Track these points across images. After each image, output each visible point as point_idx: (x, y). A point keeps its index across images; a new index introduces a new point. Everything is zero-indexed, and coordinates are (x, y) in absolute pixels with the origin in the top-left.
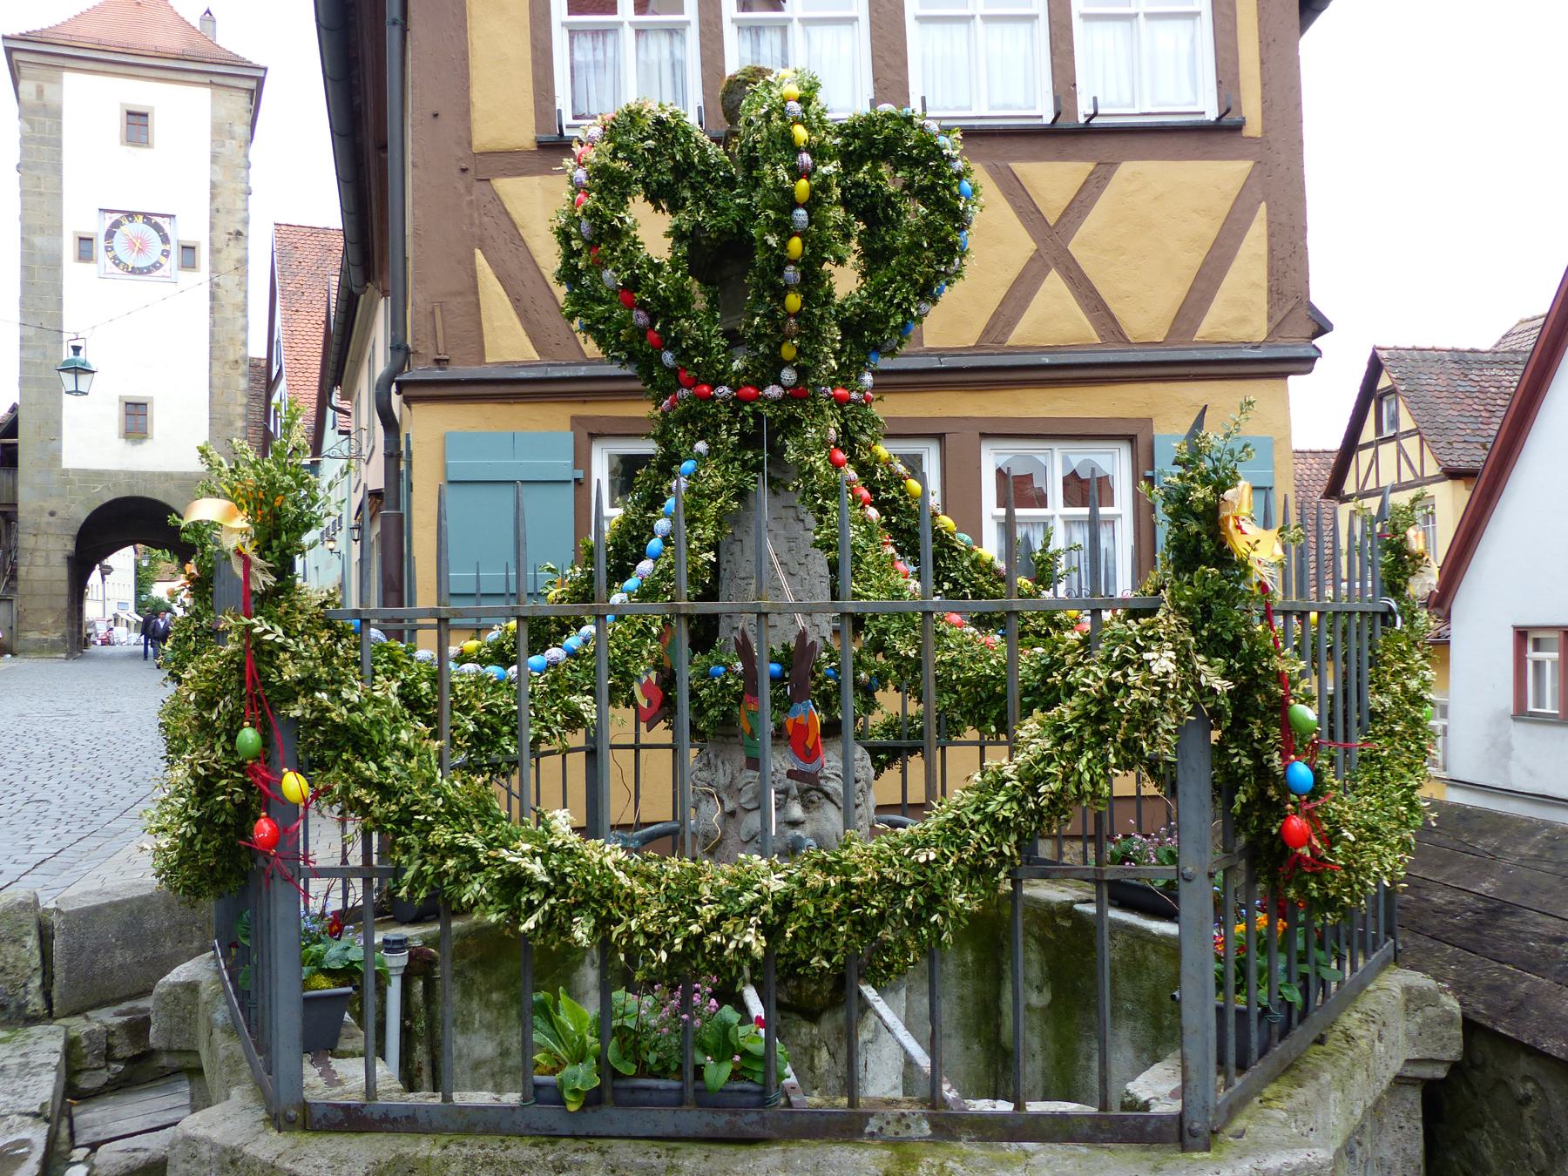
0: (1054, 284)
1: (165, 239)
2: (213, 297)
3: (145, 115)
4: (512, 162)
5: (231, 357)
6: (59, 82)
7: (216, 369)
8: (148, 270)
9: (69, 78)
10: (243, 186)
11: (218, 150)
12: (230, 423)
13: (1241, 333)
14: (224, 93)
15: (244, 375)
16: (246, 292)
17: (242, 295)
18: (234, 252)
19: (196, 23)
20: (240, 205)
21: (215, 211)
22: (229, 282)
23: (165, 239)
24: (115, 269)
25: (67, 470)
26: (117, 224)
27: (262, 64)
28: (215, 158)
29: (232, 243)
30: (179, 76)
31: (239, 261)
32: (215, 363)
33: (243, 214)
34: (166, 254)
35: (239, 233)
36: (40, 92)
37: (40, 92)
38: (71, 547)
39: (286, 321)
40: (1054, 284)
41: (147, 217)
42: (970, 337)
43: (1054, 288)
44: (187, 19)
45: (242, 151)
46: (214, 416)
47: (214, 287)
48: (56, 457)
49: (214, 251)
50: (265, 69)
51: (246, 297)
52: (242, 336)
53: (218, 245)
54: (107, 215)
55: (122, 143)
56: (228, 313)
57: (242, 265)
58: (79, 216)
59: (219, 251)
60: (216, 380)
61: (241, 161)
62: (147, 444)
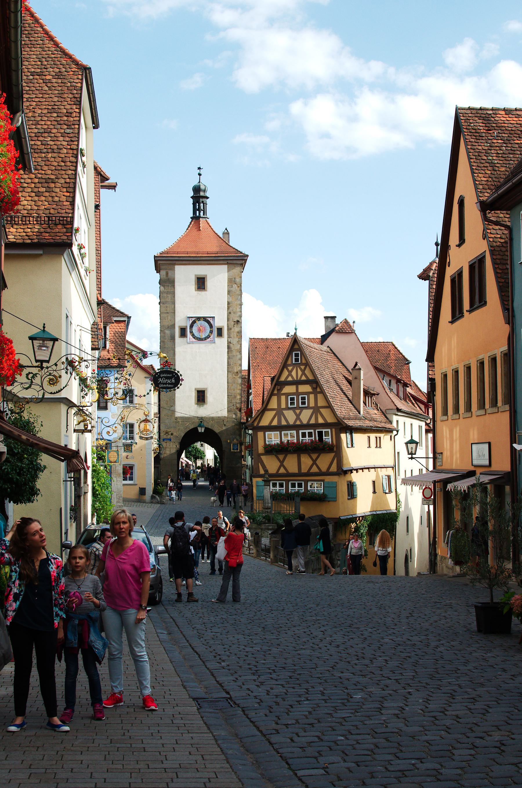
0: (315, 466)
1: (211, 326)
2: (229, 347)
3: (204, 278)
4: (262, 454)
5: (236, 371)
6: (174, 270)
7: (230, 376)
8: (205, 339)
9: (177, 267)
10: (239, 302)
11: (230, 289)
12: (235, 397)
13: (334, 471)
14: (231, 266)
15: (240, 377)
16: (241, 344)
17: (239, 346)
18: (236, 329)
19: (221, 236)
20: (238, 310)
21: (229, 313)
22: (235, 341)
23: (211, 326)
24: (194, 340)
25: (177, 418)
26: (194, 322)
27: (246, 254)
28: (229, 292)
29: (235, 326)
30: (216, 262)
31: (238, 332)
32: (229, 373)
33: (240, 313)
34: (211, 332)
35: (238, 321)
36: (167, 274)
37: (167, 274)
38: (178, 446)
39: (253, 377)
40: (315, 466)
41: (205, 319)
42: (306, 471)
43: (315, 466)
44: (218, 234)
45: (239, 289)
46: (229, 394)
47: (229, 343)
48: (174, 411)
49: (229, 329)
50: (247, 256)
51: (241, 346)
52: (239, 362)
53: (230, 327)
54: (191, 319)
55: (195, 290)
56: (234, 353)
57: (240, 333)
58: (181, 320)
59: (231, 329)
60: (230, 380)
61: (238, 292)
62: (205, 406)
